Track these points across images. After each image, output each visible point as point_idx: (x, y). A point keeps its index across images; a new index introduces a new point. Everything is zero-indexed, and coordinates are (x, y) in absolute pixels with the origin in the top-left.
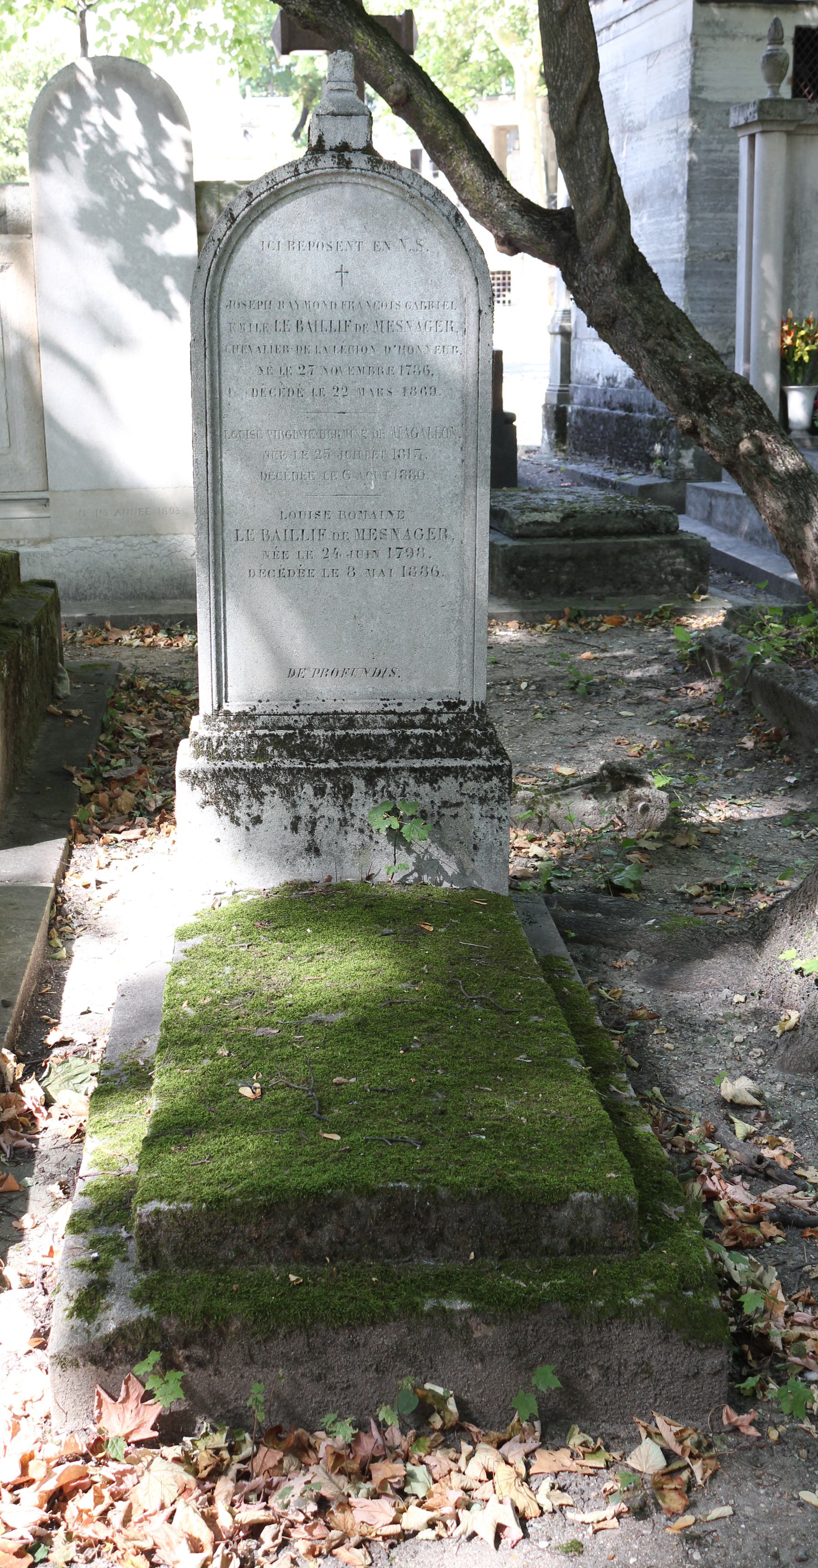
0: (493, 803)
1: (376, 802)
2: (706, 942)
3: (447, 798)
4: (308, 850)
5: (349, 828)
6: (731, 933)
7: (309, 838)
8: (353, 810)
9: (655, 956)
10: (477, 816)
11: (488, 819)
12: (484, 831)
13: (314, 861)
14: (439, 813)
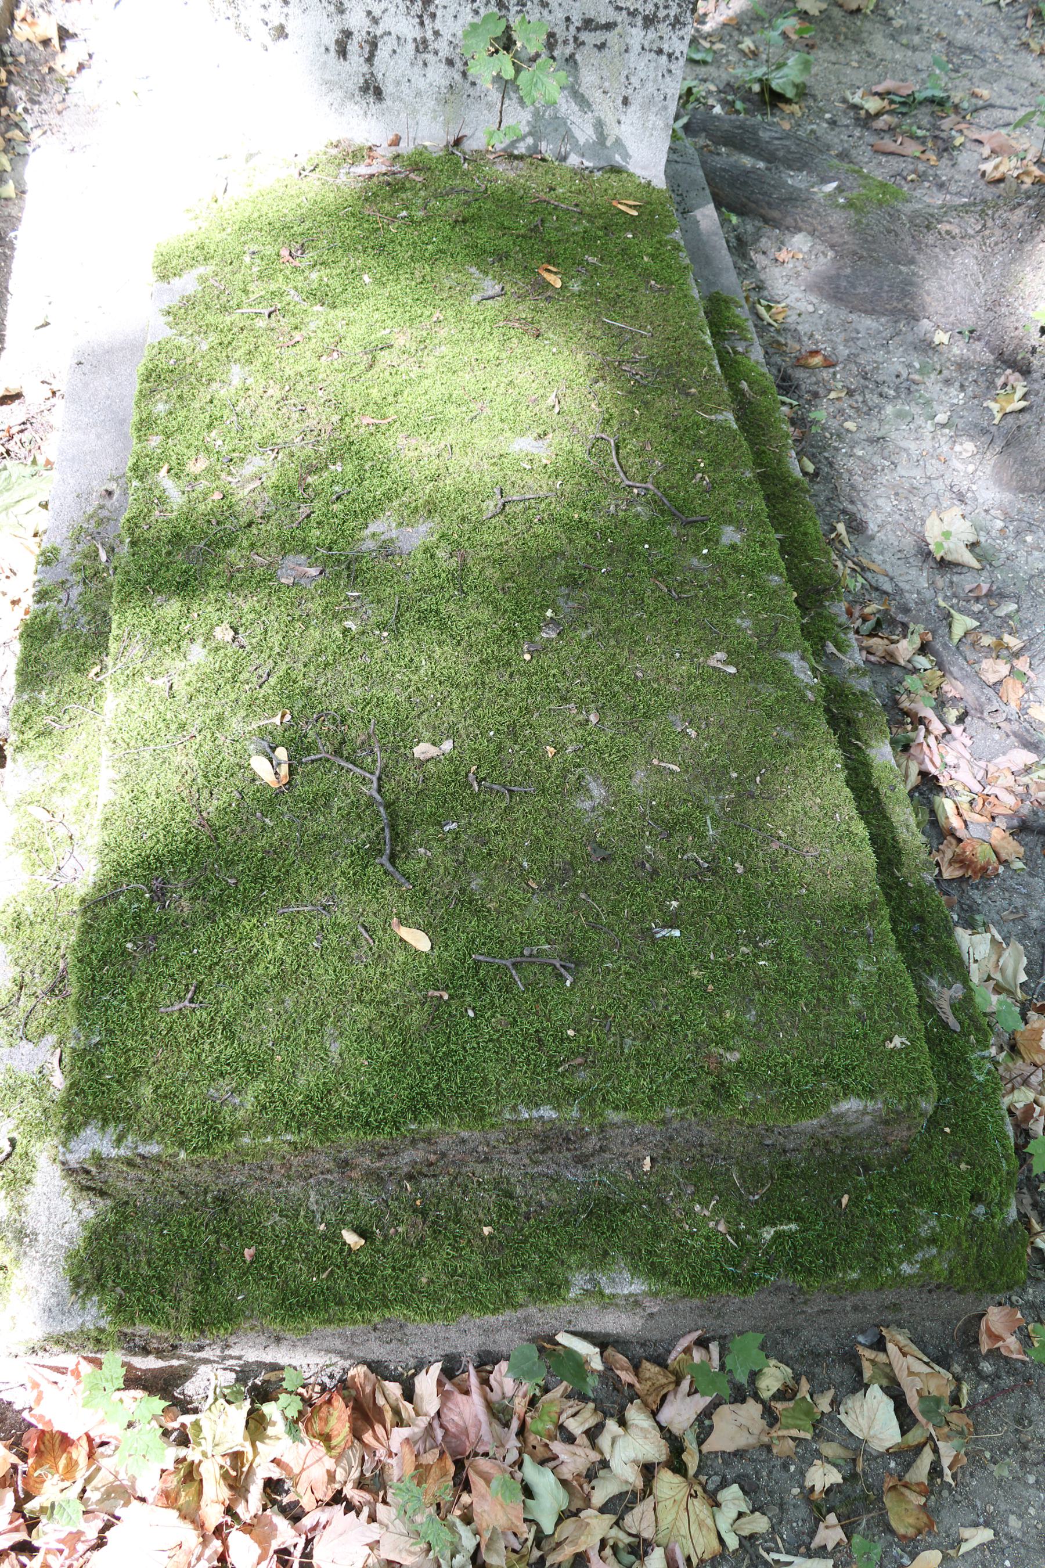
0: (664, 28)
1: (476, 12)
2: (908, 239)
3: (591, 14)
4: (365, 89)
5: (429, 57)
6: (948, 233)
7: (365, 68)
8: (438, 25)
9: (832, 246)
10: (636, 48)
11: (653, 55)
12: (642, 75)
13: (374, 108)
14: (576, 39)
